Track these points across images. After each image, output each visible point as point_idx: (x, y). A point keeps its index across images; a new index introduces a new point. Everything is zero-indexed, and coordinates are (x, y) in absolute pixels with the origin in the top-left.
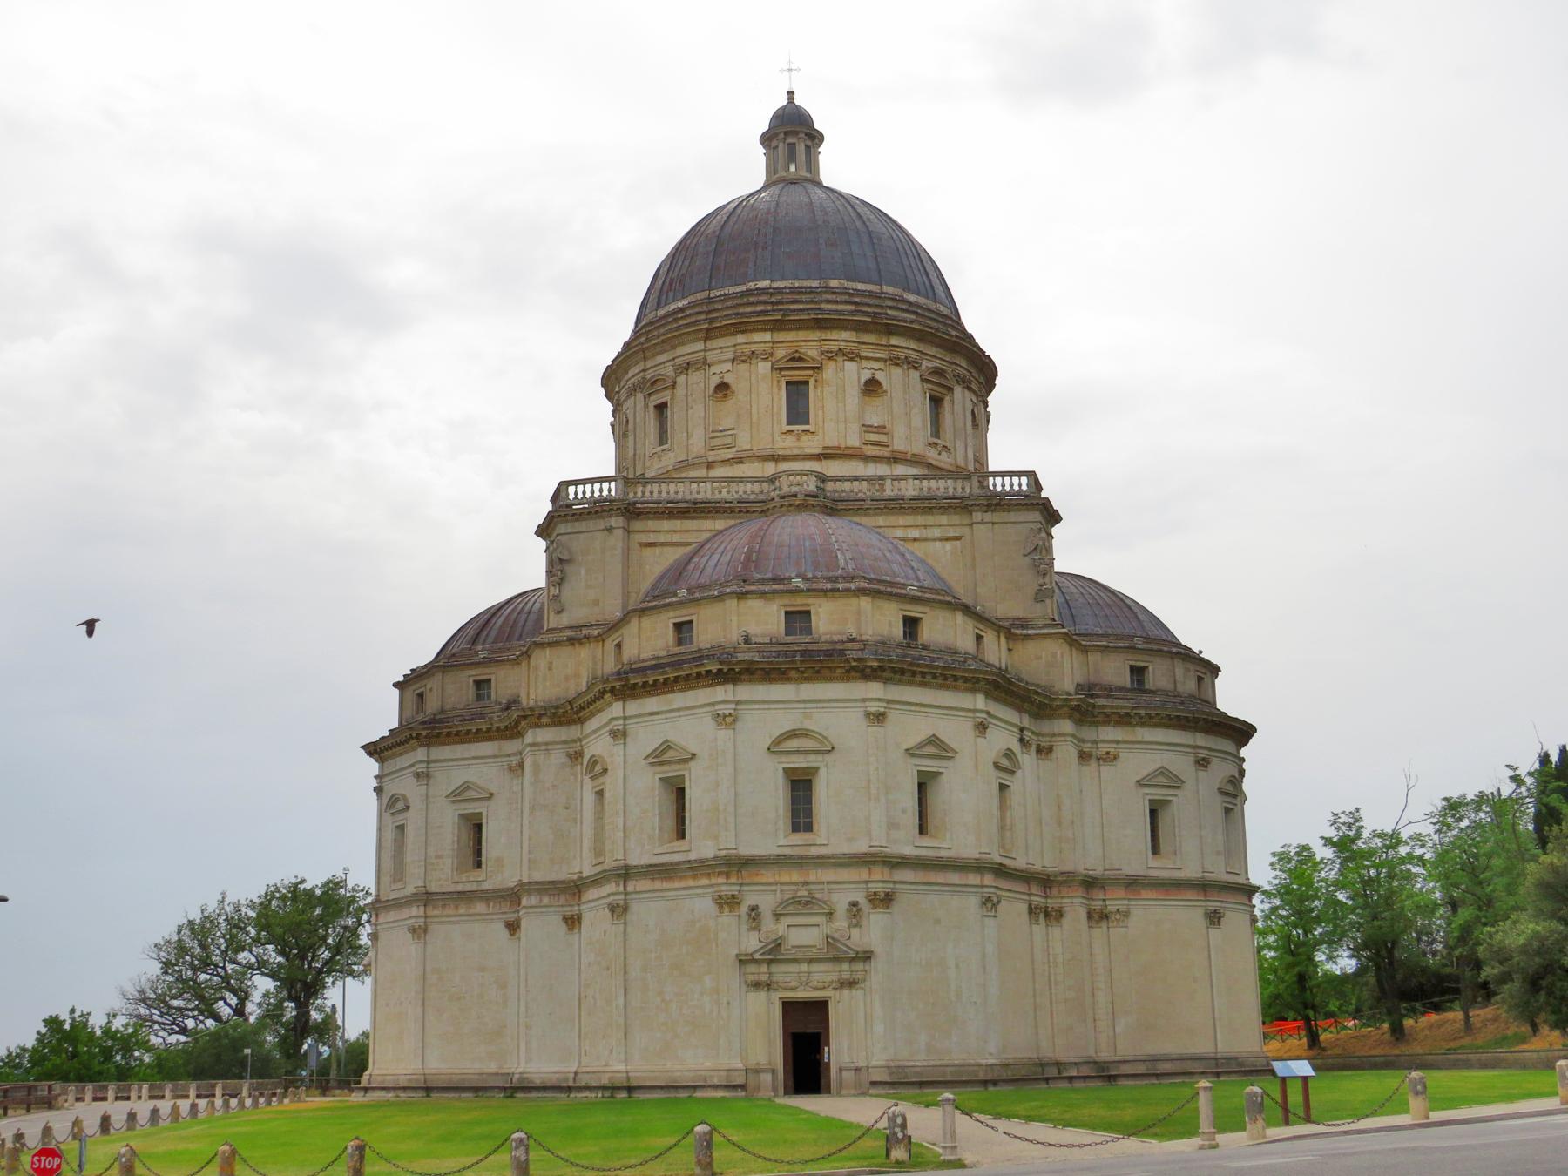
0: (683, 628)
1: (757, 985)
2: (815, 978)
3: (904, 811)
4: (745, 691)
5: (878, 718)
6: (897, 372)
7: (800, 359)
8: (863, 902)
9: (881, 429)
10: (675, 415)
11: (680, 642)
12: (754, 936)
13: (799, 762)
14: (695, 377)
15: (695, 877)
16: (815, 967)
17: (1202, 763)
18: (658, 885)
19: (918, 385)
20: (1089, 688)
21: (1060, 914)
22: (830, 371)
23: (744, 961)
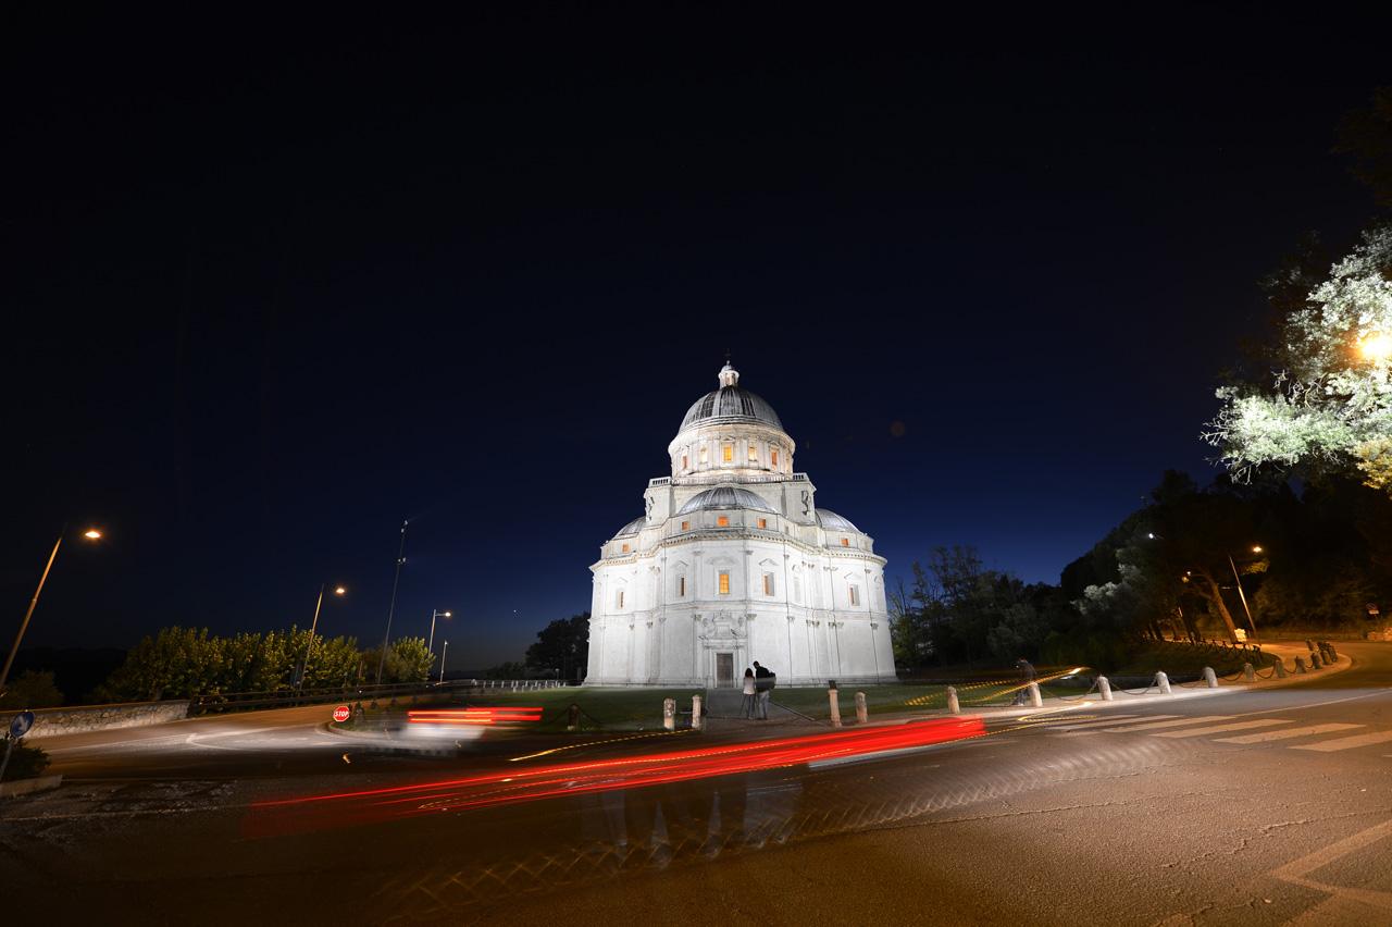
1: (708, 647)
4: (704, 543)
10: (689, 461)
12: (706, 629)
17: (867, 571)
22: (738, 443)
23: (703, 637)
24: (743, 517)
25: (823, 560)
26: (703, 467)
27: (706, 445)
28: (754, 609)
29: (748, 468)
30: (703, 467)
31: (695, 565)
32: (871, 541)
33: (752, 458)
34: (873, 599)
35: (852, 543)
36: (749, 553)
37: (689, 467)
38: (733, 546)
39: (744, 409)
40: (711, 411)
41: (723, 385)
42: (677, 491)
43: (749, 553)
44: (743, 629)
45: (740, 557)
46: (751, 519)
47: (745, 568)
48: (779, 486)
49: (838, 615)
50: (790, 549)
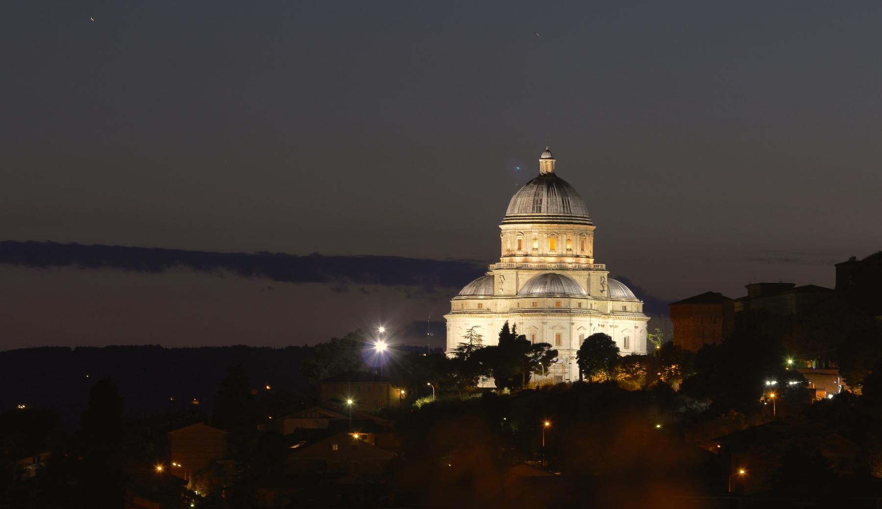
4: (548, 317)
5: (573, 324)
10: (523, 244)
14: (528, 235)
17: (636, 327)
20: (613, 312)
22: (560, 238)
24: (569, 303)
25: (611, 321)
26: (535, 253)
29: (566, 256)
30: (535, 253)
31: (543, 330)
33: (568, 247)
34: (638, 344)
35: (628, 309)
36: (573, 324)
38: (563, 320)
40: (540, 208)
42: (521, 272)
45: (567, 326)
46: (574, 303)
48: (586, 273)
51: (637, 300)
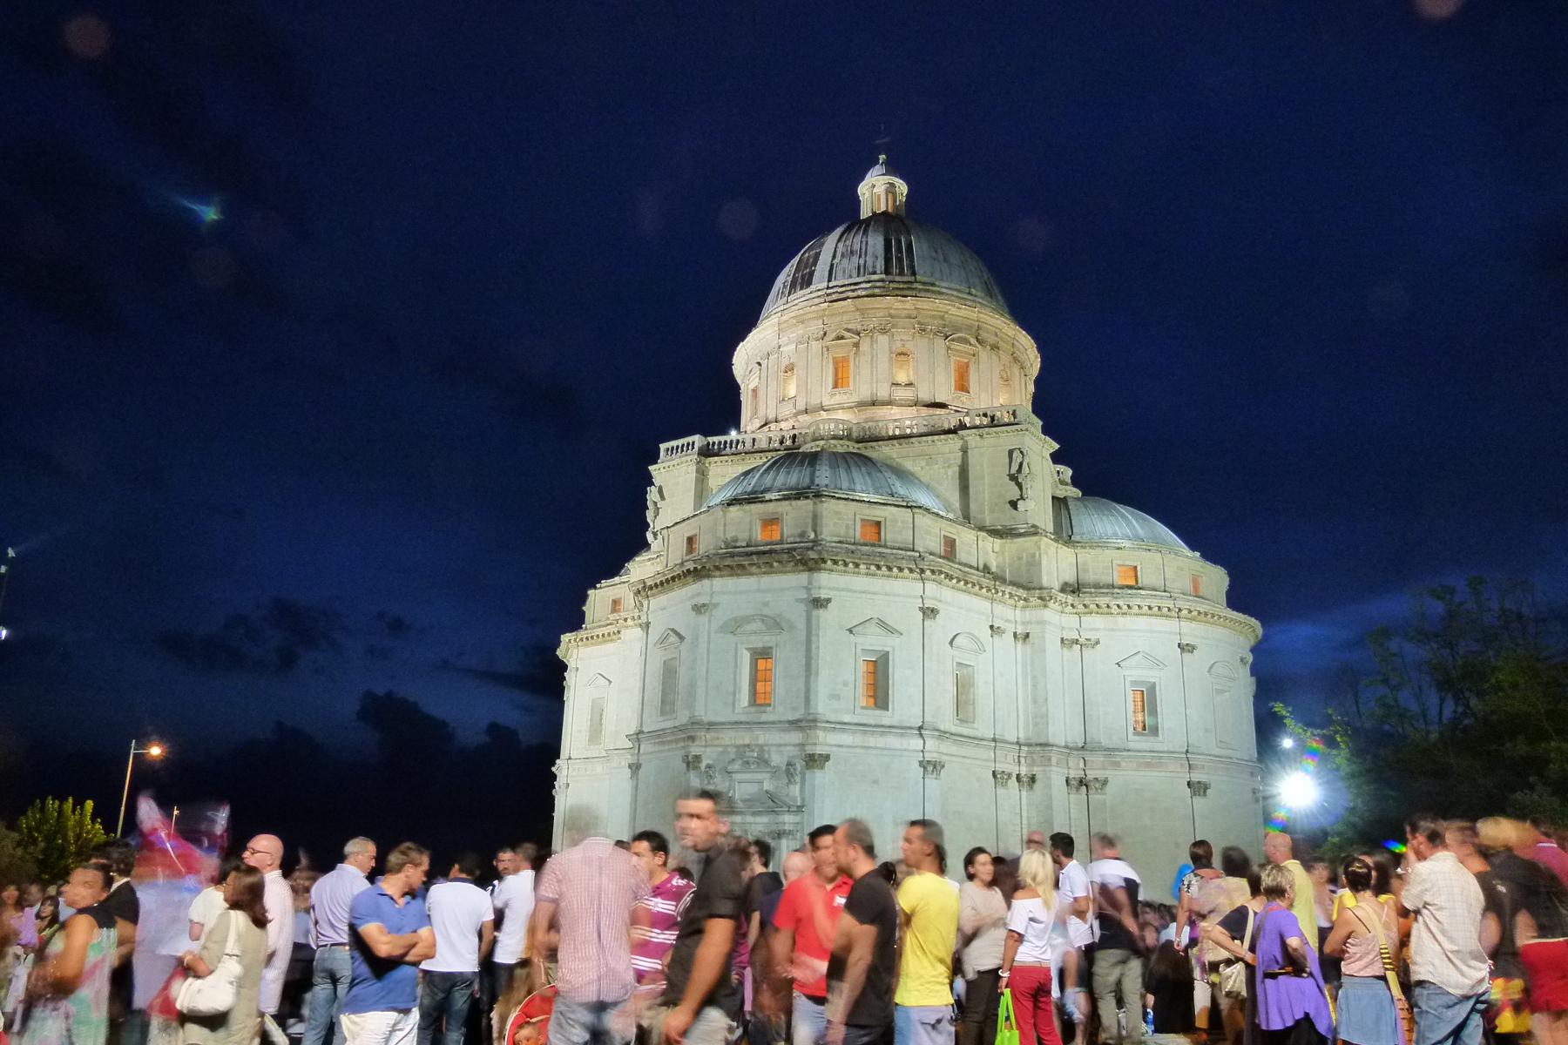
0: (690, 540)
2: (760, 828)
3: (846, 685)
6: (923, 342)
7: (842, 338)
8: (799, 765)
9: (910, 384)
10: (761, 394)
11: (690, 549)
13: (758, 643)
15: (677, 741)
16: (759, 819)
17: (1185, 648)
18: (657, 748)
19: (943, 351)
21: (1033, 779)
22: (865, 345)
24: (816, 520)
25: (1058, 619)
26: (787, 410)
27: (794, 359)
28: (825, 741)
29: (889, 403)
32: (1216, 579)
33: (902, 378)
36: (819, 603)
37: (761, 413)
39: (888, 260)
40: (811, 274)
41: (865, 213)
43: (819, 603)
44: (795, 790)
45: (797, 614)
47: (809, 642)
48: (952, 444)
49: (1096, 759)
50: (938, 593)
51: (1189, 553)
